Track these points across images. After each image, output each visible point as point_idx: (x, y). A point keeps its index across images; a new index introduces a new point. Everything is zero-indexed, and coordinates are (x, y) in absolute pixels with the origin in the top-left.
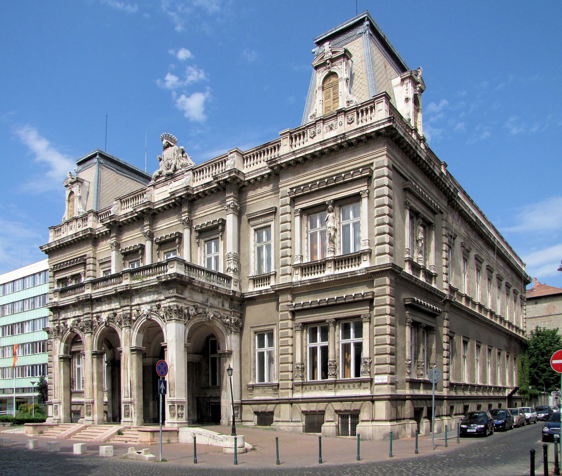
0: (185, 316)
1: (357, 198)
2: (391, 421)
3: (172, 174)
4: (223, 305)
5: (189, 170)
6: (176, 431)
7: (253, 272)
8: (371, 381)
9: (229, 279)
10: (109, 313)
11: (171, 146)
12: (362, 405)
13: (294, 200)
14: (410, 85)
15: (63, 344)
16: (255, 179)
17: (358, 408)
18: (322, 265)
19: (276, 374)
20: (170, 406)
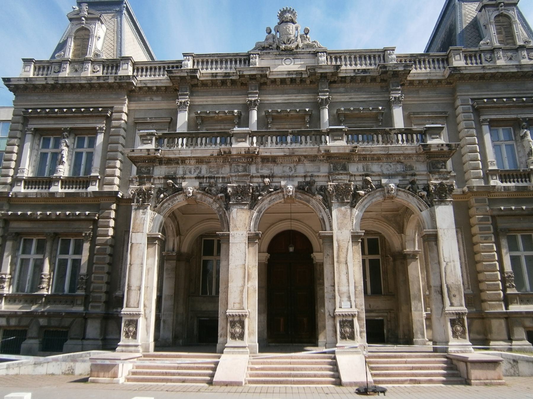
13: (477, 111)
16: (421, 82)
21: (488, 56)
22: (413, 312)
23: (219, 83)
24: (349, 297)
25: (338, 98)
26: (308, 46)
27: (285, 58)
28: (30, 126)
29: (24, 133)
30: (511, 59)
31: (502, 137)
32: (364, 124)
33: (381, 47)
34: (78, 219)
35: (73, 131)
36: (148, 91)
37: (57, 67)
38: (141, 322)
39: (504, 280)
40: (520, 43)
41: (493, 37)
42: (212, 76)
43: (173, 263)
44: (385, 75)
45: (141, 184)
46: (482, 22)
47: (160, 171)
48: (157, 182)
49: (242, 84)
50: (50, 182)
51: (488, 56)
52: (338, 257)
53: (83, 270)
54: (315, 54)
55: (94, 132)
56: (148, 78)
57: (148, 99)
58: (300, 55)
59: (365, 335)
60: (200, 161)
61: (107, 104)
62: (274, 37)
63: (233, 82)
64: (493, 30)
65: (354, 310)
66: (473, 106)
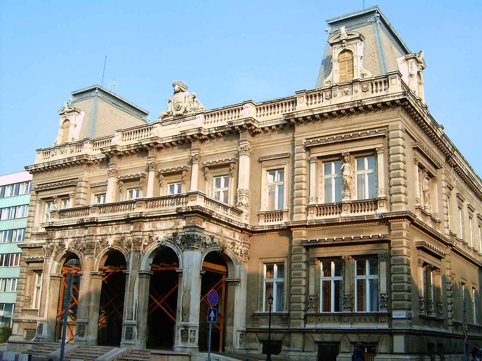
0: (202, 244)
1: (373, 153)
2: (409, 354)
3: (181, 115)
4: (234, 237)
5: (201, 113)
6: (188, 355)
7: (265, 207)
8: (389, 315)
9: (240, 213)
10: (115, 236)
11: (182, 91)
12: (379, 338)
14: (414, 64)
15: (56, 263)
16: (270, 127)
17: (376, 341)
18: (340, 206)
19: (285, 304)
20: (182, 330)
21: (328, 94)
27: (177, 122)
30: (347, 94)
32: (221, 173)
39: (306, 303)
42: (128, 148)
48: (56, 241)
58: (187, 118)
61: (71, 177)
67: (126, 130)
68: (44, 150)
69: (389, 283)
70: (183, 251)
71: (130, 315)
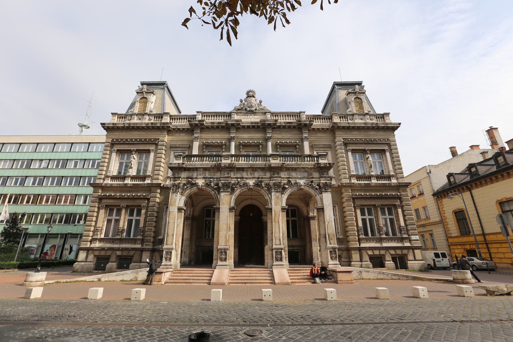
13: (346, 144)
15: (184, 198)
16: (318, 129)
21: (351, 117)
22: (313, 247)
23: (215, 127)
24: (280, 240)
25: (276, 136)
26: (262, 109)
28: (114, 148)
29: (111, 152)
31: (358, 159)
33: (298, 111)
34: (139, 198)
35: (137, 151)
36: (178, 130)
37: (130, 118)
38: (174, 252)
39: (358, 231)
40: (366, 112)
41: (353, 108)
43: (190, 221)
44: (301, 126)
45: (174, 181)
46: (348, 101)
47: (184, 175)
49: (227, 128)
50: (124, 178)
51: (351, 117)
52: (275, 219)
53: (141, 225)
54: (265, 113)
55: (148, 151)
56: (178, 124)
57: (178, 134)
59: (287, 259)
60: (205, 169)
62: (244, 104)
63: (223, 127)
64: (353, 104)
65: (282, 246)
66: (343, 142)
67: (205, 113)
68: (118, 115)
69: (405, 221)
70: (321, 193)
71: (278, 241)
